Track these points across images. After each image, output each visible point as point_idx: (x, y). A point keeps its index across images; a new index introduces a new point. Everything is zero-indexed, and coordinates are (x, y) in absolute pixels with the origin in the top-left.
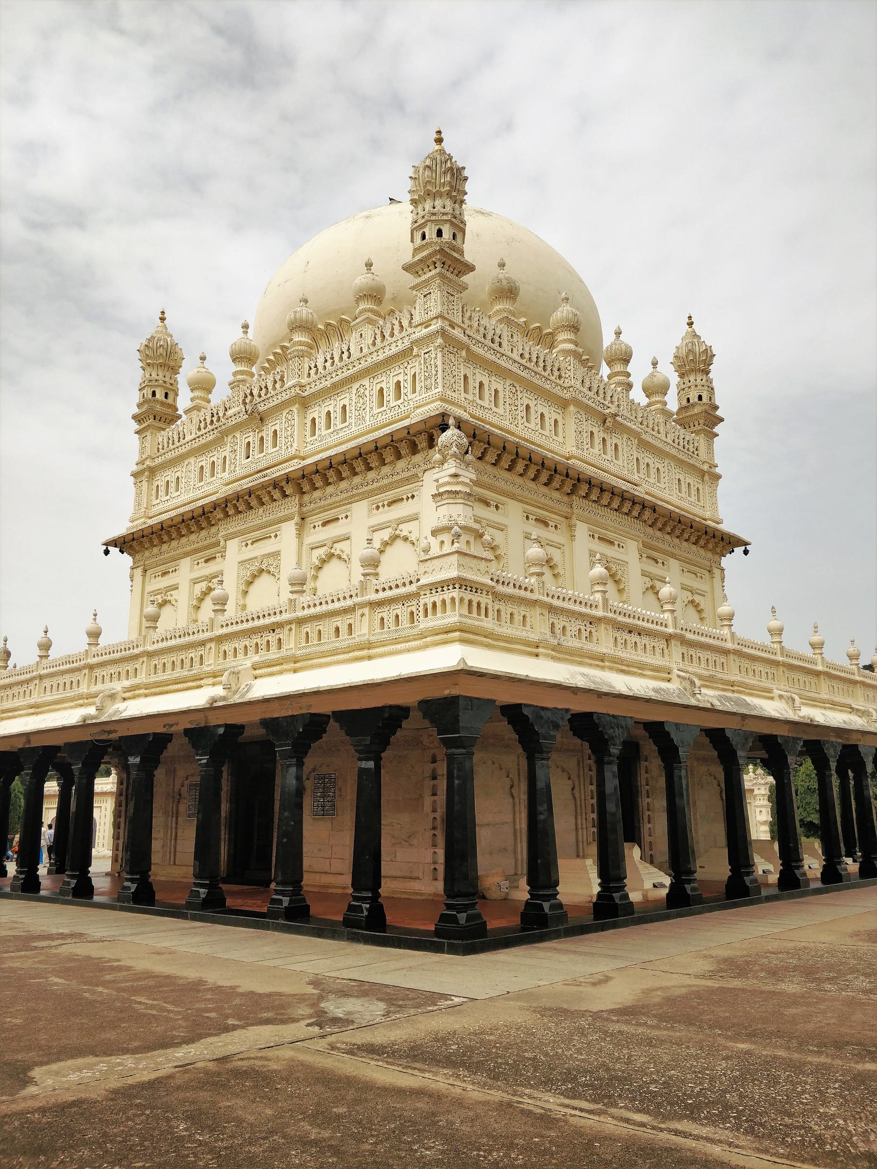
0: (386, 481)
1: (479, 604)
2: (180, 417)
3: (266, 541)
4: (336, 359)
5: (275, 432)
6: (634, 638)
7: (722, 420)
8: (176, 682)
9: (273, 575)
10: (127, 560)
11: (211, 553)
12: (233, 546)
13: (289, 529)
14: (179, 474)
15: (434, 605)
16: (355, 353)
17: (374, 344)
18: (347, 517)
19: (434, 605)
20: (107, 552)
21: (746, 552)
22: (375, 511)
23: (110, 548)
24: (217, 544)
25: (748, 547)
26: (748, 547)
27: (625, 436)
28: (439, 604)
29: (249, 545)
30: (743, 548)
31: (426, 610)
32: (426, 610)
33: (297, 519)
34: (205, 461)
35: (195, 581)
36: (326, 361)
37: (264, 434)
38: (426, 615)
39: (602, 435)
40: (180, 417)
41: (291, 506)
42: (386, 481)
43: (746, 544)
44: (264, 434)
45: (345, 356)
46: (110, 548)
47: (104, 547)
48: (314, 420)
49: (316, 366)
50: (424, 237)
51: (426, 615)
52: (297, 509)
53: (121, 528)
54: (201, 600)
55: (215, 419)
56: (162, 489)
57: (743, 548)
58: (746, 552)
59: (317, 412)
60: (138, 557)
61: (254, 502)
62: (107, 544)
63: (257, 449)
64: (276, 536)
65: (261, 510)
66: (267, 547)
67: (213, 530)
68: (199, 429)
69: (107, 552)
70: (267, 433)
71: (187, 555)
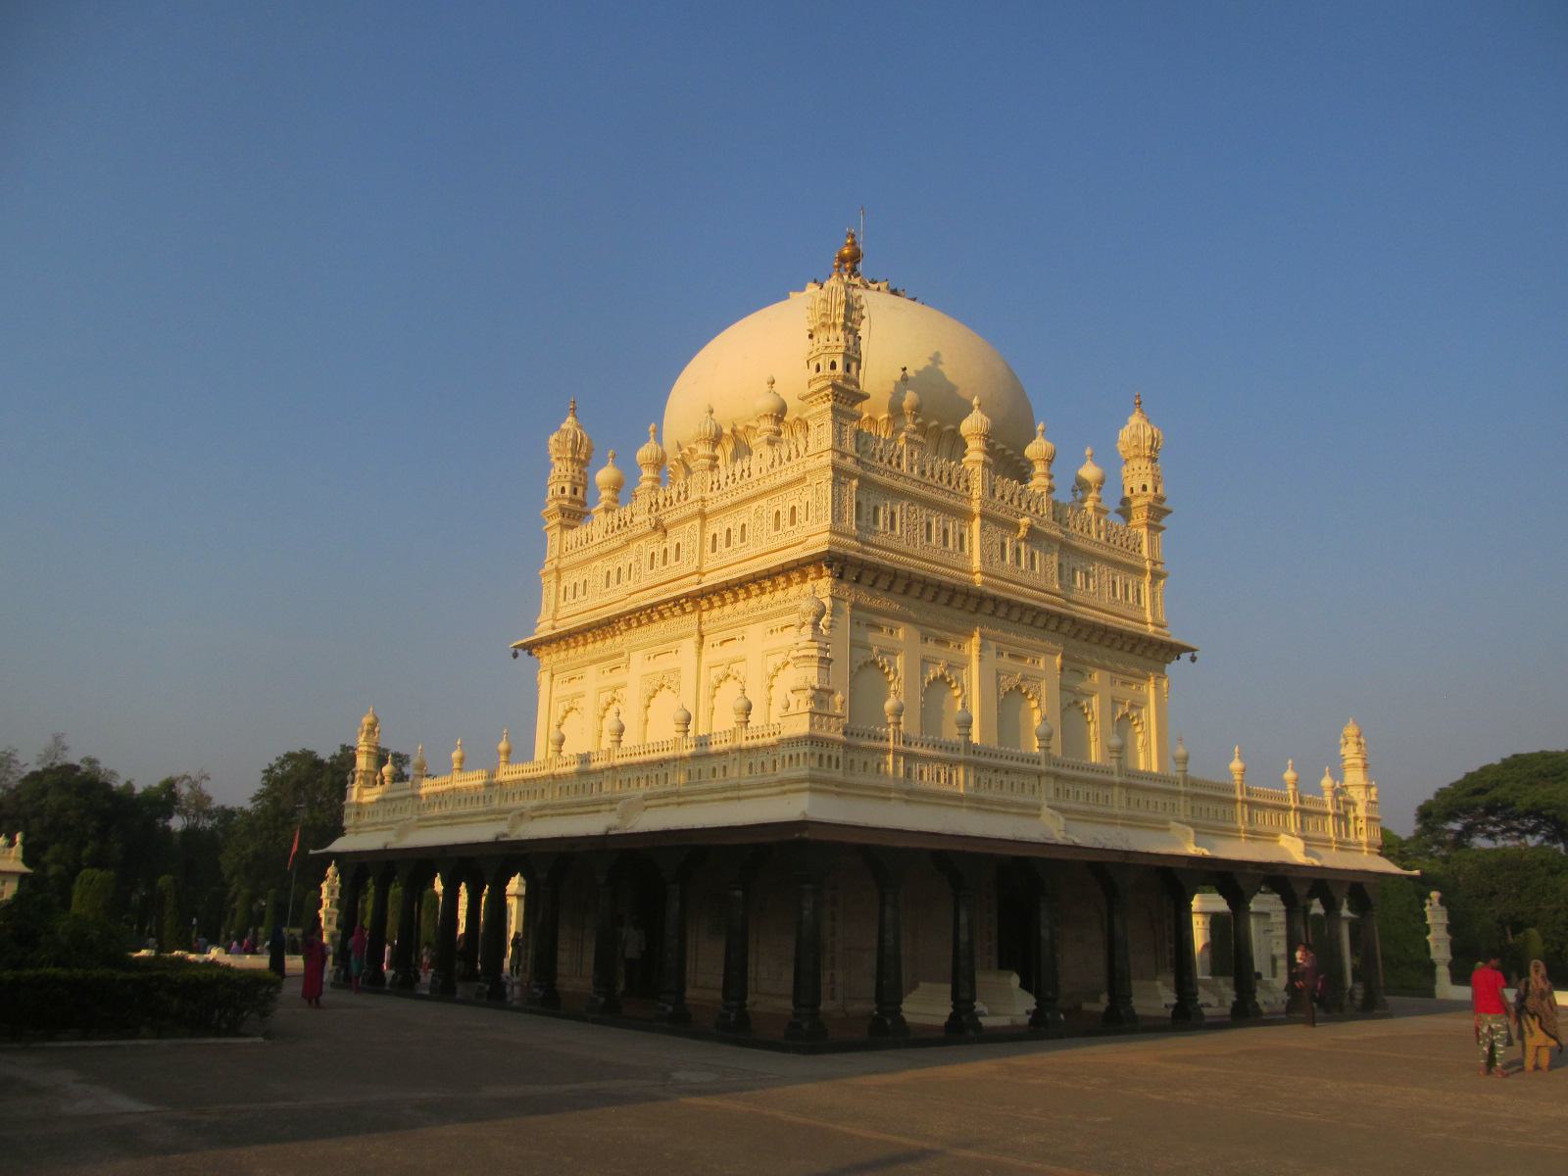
0: (778, 607)
1: (830, 757)
4: (738, 476)
5: (678, 545)
6: (1000, 777)
7: (1170, 512)
8: (579, 805)
11: (615, 662)
12: (637, 657)
13: (690, 644)
14: (586, 577)
16: (756, 474)
17: (772, 466)
18: (743, 638)
20: (515, 655)
21: (1193, 659)
22: (769, 635)
23: (519, 651)
25: (1196, 654)
26: (1196, 654)
33: (696, 637)
34: (611, 565)
36: (728, 477)
42: (778, 607)
43: (1193, 650)
45: (746, 474)
46: (519, 651)
47: (513, 650)
49: (718, 481)
50: (818, 369)
55: (622, 524)
57: (1190, 654)
58: (1193, 659)
61: (656, 617)
63: (661, 562)
65: (663, 625)
68: (607, 532)
69: (515, 655)
70: (670, 545)
71: (594, 662)
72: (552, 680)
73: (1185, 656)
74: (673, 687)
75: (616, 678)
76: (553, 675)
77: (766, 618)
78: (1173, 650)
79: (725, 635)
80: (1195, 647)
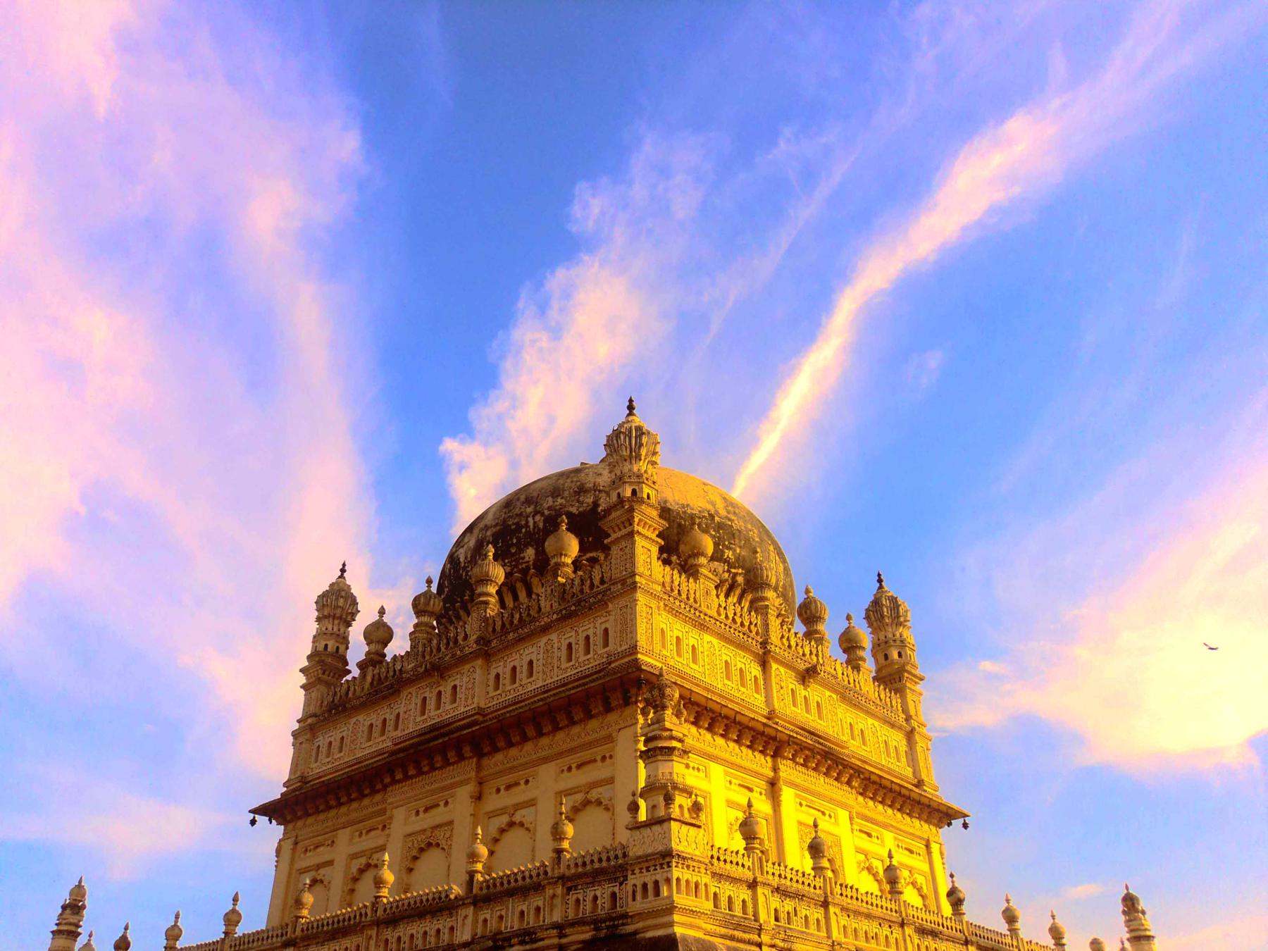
2: (349, 672)
3: (590, 766)
5: (455, 687)
9: (527, 829)
10: (277, 831)
12: (399, 815)
13: (464, 794)
15: (645, 886)
19: (645, 886)
20: (253, 822)
21: (965, 826)
24: (383, 812)
27: (828, 693)
28: (650, 887)
29: (574, 769)
30: (962, 820)
31: (634, 892)
32: (634, 892)
35: (354, 856)
37: (441, 688)
38: (634, 899)
39: (804, 693)
40: (349, 672)
41: (467, 769)
44: (441, 688)
48: (498, 676)
51: (634, 899)
52: (473, 774)
53: (275, 792)
54: (355, 880)
56: (324, 750)
57: (962, 820)
58: (965, 826)
59: (502, 667)
60: (290, 826)
62: (254, 811)
64: (446, 803)
66: (439, 815)
67: (378, 797)
69: (253, 822)
70: (446, 689)
72: (294, 850)
73: (957, 823)
74: (443, 843)
75: (368, 843)
76: (296, 843)
77: (560, 755)
78: (942, 815)
79: (509, 779)
80: (966, 812)
